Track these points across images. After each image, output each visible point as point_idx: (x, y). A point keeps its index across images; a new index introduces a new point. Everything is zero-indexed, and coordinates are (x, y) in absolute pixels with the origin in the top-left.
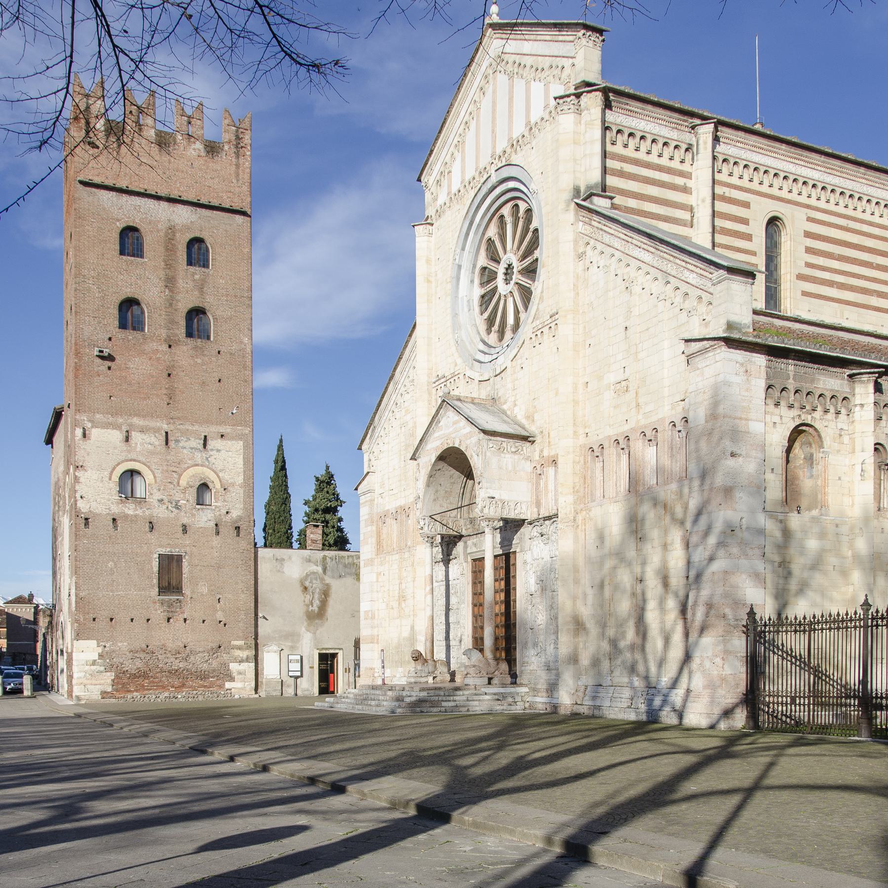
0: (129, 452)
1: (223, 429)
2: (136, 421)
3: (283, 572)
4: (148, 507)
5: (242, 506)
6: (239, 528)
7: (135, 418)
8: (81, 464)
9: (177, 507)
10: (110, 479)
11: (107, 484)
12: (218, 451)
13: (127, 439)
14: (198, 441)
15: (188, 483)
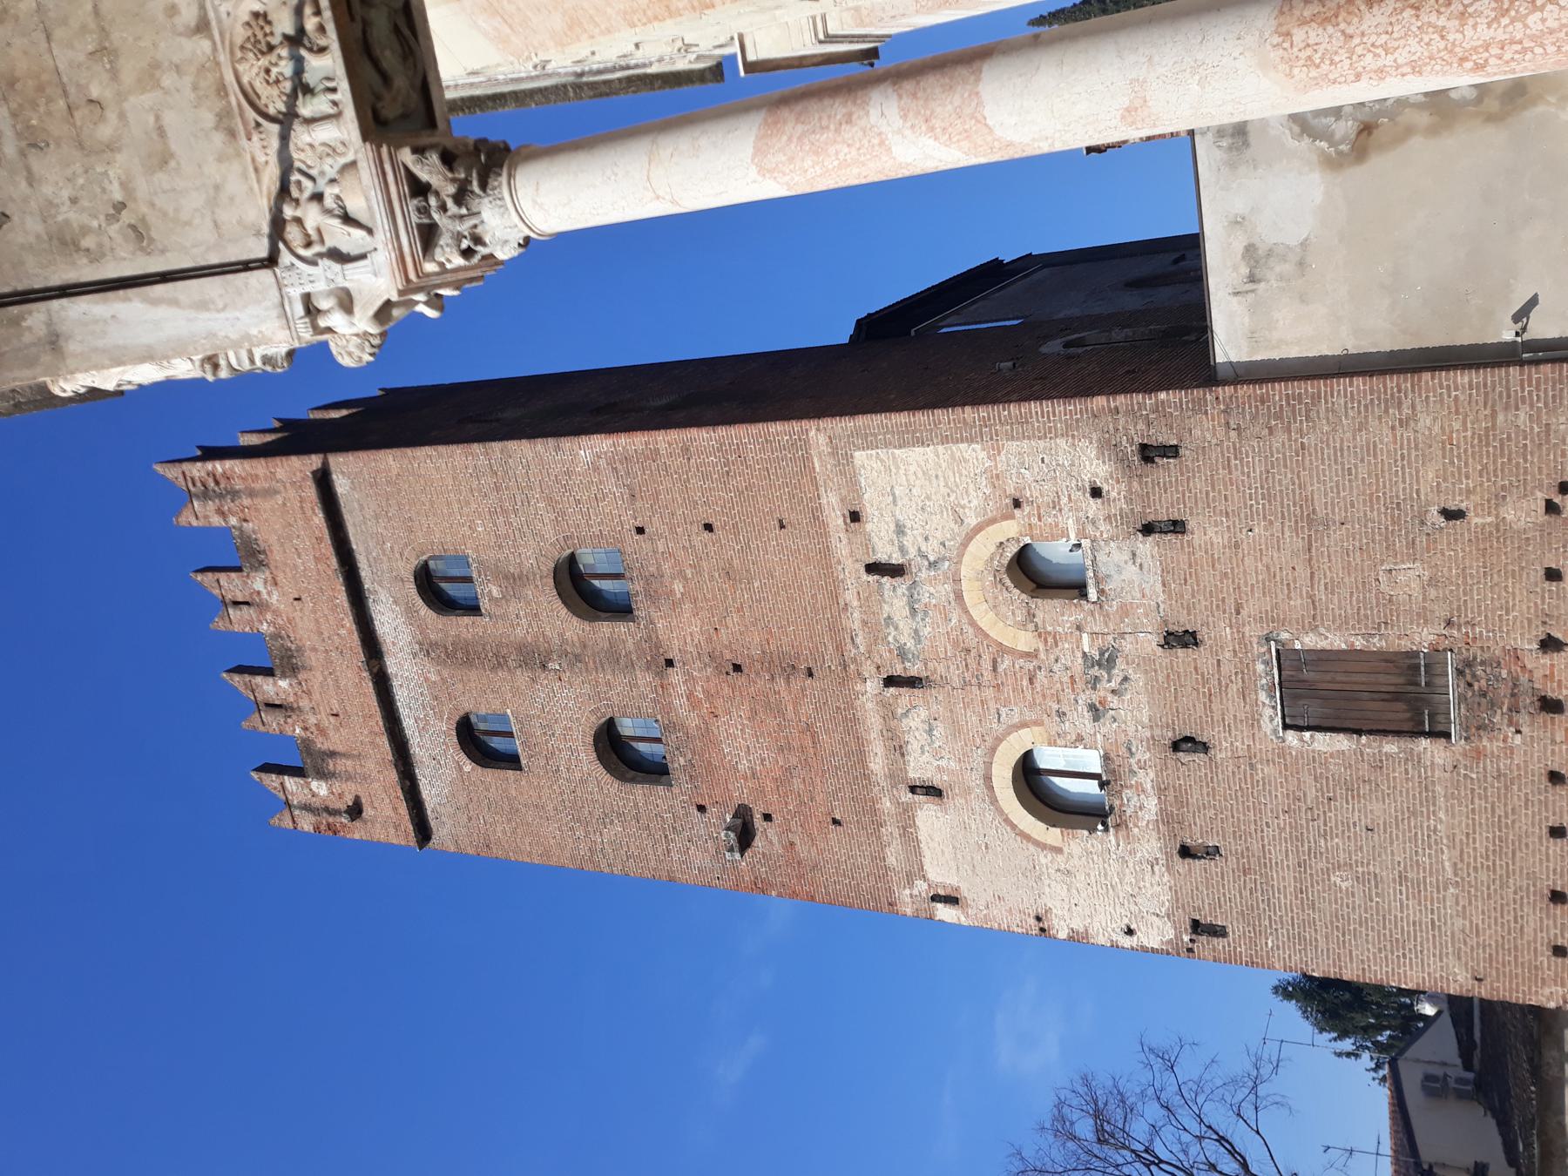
0: (967, 791)
1: (836, 519)
2: (878, 764)
3: (1304, 244)
4: (1123, 751)
5: (1061, 442)
6: (1144, 448)
7: (872, 765)
8: (1032, 921)
9: (1107, 660)
10: (1059, 850)
11: (1076, 861)
12: (900, 530)
13: (933, 792)
14: (887, 593)
15: (1023, 626)
